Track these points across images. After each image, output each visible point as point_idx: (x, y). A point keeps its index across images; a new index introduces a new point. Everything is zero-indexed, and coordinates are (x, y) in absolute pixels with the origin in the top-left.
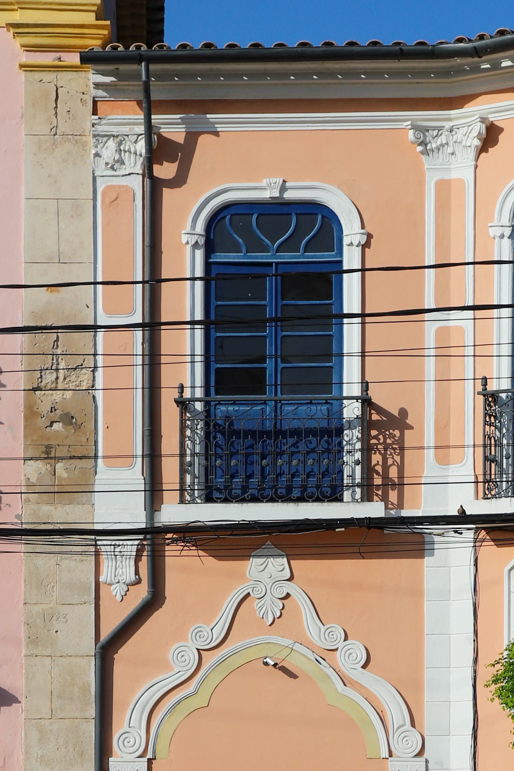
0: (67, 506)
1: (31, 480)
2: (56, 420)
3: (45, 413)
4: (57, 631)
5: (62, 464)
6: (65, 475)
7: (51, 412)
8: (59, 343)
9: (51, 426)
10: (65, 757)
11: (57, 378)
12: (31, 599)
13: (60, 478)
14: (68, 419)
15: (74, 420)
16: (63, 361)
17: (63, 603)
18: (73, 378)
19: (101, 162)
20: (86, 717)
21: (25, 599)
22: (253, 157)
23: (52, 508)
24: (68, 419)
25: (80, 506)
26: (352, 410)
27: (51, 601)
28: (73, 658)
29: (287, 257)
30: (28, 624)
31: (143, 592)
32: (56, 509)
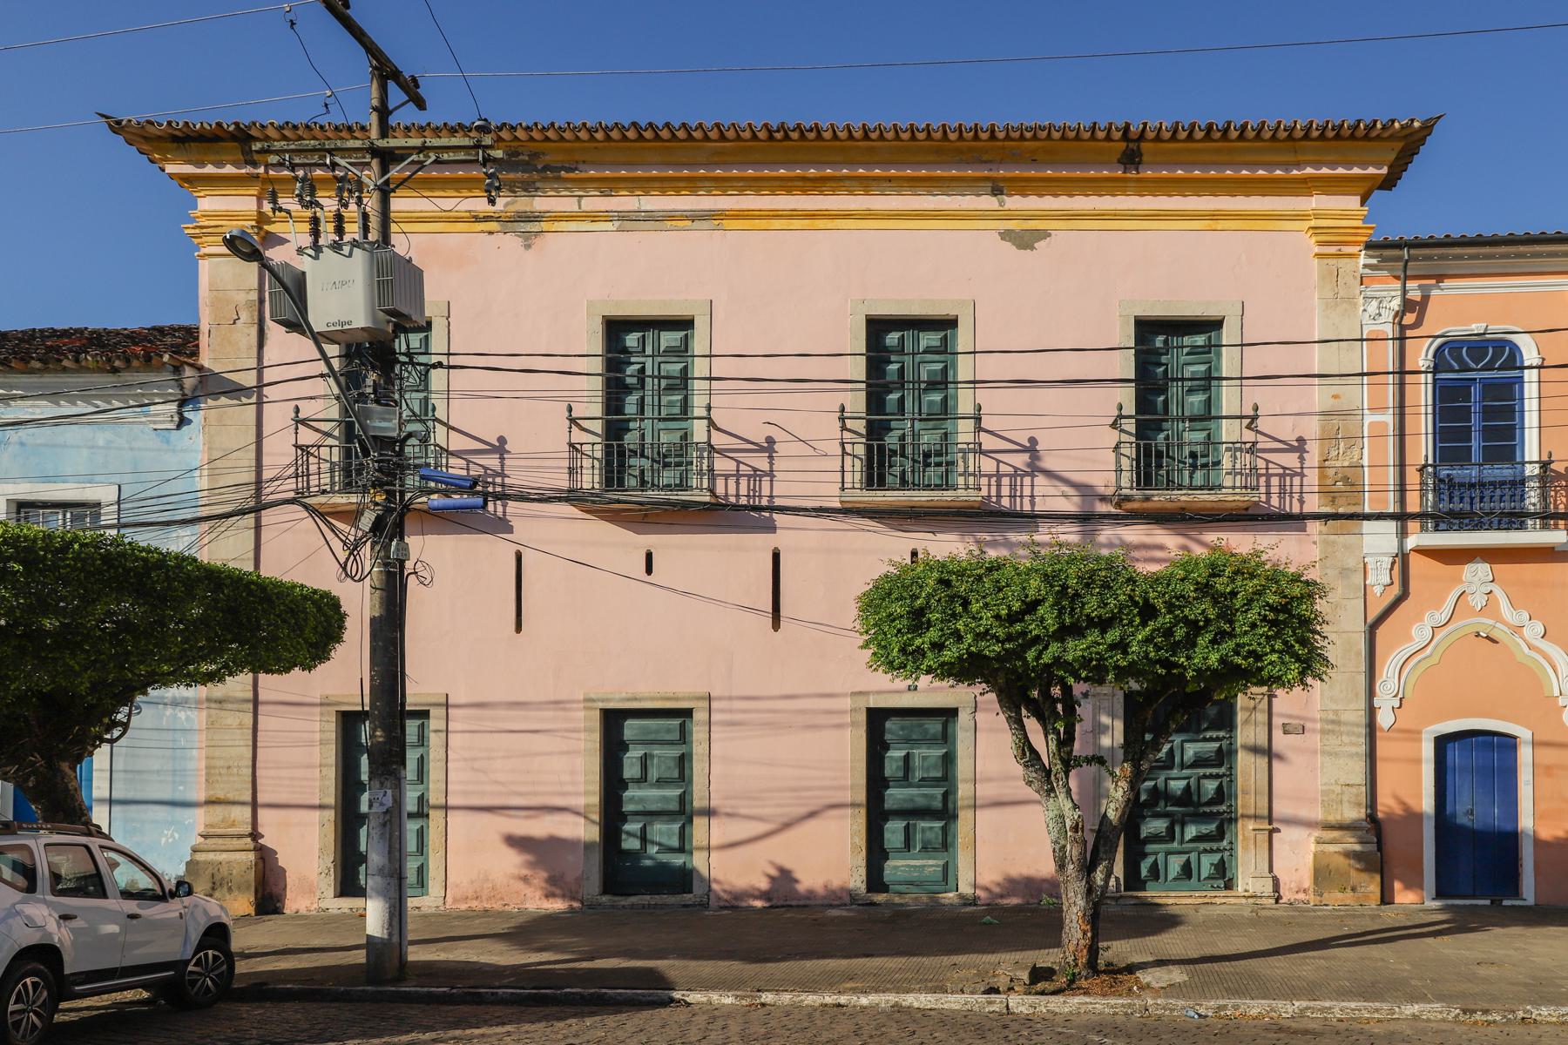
19: (1366, 315)
22: (1468, 305)
26: (1532, 470)
29: (1486, 374)
31: (1396, 590)
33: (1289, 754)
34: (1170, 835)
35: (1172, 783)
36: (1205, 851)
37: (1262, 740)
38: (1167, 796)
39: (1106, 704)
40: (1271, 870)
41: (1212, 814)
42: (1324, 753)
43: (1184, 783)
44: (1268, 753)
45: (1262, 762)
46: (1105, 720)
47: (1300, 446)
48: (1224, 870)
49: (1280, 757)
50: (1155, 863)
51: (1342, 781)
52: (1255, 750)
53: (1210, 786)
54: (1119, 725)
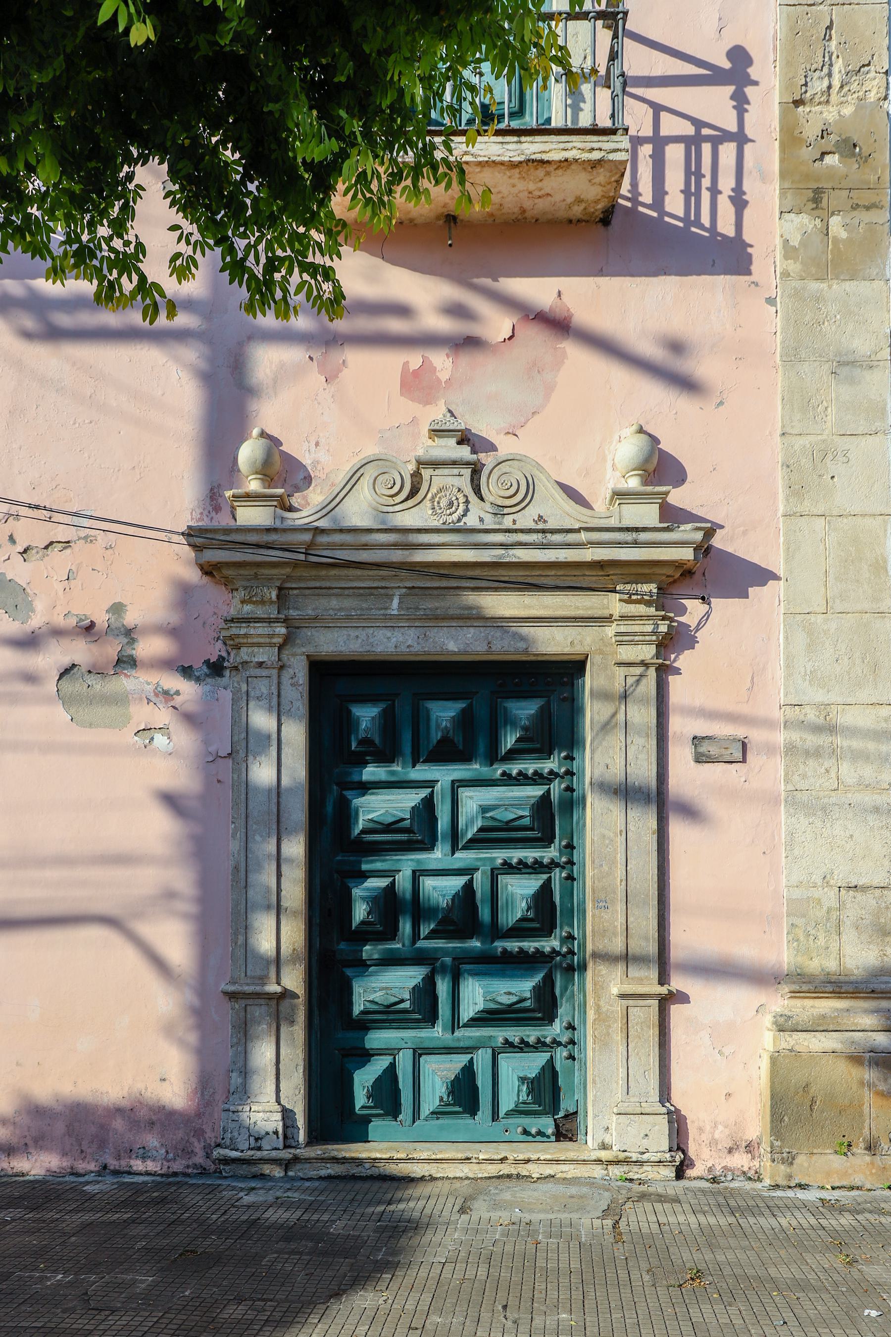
0: (848, 283)
1: (791, 243)
2: (829, 150)
3: (812, 139)
4: (833, 477)
5: (839, 218)
6: (844, 235)
7: (822, 137)
8: (833, 32)
9: (821, 159)
10: (849, 673)
11: (830, 87)
12: (792, 427)
13: (836, 240)
14: (849, 148)
15: (858, 149)
16: (840, 59)
17: (841, 433)
18: (854, 86)
20: (881, 610)
21: (783, 426)
23: (824, 286)
24: (849, 148)
25: (867, 283)
27: (823, 430)
28: (859, 519)
30: (788, 466)
32: (830, 287)
33: (711, 805)
34: (424, 1007)
35: (429, 884)
36: (508, 1044)
37: (644, 771)
38: (419, 909)
39: (262, 687)
40: (665, 1094)
41: (534, 952)
42: (792, 802)
43: (458, 882)
44: (658, 799)
45: (644, 822)
46: (262, 720)
47: (736, 72)
48: (556, 1091)
49: (690, 812)
50: (391, 1072)
51: (839, 879)
52: (625, 792)
53: (520, 891)
54: (296, 734)
